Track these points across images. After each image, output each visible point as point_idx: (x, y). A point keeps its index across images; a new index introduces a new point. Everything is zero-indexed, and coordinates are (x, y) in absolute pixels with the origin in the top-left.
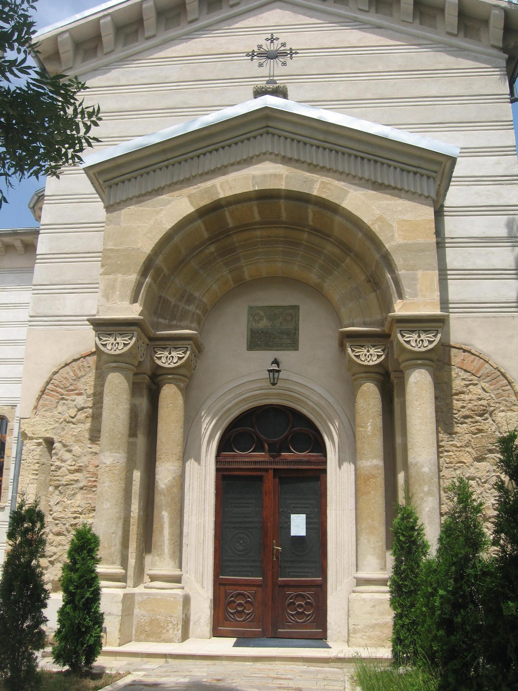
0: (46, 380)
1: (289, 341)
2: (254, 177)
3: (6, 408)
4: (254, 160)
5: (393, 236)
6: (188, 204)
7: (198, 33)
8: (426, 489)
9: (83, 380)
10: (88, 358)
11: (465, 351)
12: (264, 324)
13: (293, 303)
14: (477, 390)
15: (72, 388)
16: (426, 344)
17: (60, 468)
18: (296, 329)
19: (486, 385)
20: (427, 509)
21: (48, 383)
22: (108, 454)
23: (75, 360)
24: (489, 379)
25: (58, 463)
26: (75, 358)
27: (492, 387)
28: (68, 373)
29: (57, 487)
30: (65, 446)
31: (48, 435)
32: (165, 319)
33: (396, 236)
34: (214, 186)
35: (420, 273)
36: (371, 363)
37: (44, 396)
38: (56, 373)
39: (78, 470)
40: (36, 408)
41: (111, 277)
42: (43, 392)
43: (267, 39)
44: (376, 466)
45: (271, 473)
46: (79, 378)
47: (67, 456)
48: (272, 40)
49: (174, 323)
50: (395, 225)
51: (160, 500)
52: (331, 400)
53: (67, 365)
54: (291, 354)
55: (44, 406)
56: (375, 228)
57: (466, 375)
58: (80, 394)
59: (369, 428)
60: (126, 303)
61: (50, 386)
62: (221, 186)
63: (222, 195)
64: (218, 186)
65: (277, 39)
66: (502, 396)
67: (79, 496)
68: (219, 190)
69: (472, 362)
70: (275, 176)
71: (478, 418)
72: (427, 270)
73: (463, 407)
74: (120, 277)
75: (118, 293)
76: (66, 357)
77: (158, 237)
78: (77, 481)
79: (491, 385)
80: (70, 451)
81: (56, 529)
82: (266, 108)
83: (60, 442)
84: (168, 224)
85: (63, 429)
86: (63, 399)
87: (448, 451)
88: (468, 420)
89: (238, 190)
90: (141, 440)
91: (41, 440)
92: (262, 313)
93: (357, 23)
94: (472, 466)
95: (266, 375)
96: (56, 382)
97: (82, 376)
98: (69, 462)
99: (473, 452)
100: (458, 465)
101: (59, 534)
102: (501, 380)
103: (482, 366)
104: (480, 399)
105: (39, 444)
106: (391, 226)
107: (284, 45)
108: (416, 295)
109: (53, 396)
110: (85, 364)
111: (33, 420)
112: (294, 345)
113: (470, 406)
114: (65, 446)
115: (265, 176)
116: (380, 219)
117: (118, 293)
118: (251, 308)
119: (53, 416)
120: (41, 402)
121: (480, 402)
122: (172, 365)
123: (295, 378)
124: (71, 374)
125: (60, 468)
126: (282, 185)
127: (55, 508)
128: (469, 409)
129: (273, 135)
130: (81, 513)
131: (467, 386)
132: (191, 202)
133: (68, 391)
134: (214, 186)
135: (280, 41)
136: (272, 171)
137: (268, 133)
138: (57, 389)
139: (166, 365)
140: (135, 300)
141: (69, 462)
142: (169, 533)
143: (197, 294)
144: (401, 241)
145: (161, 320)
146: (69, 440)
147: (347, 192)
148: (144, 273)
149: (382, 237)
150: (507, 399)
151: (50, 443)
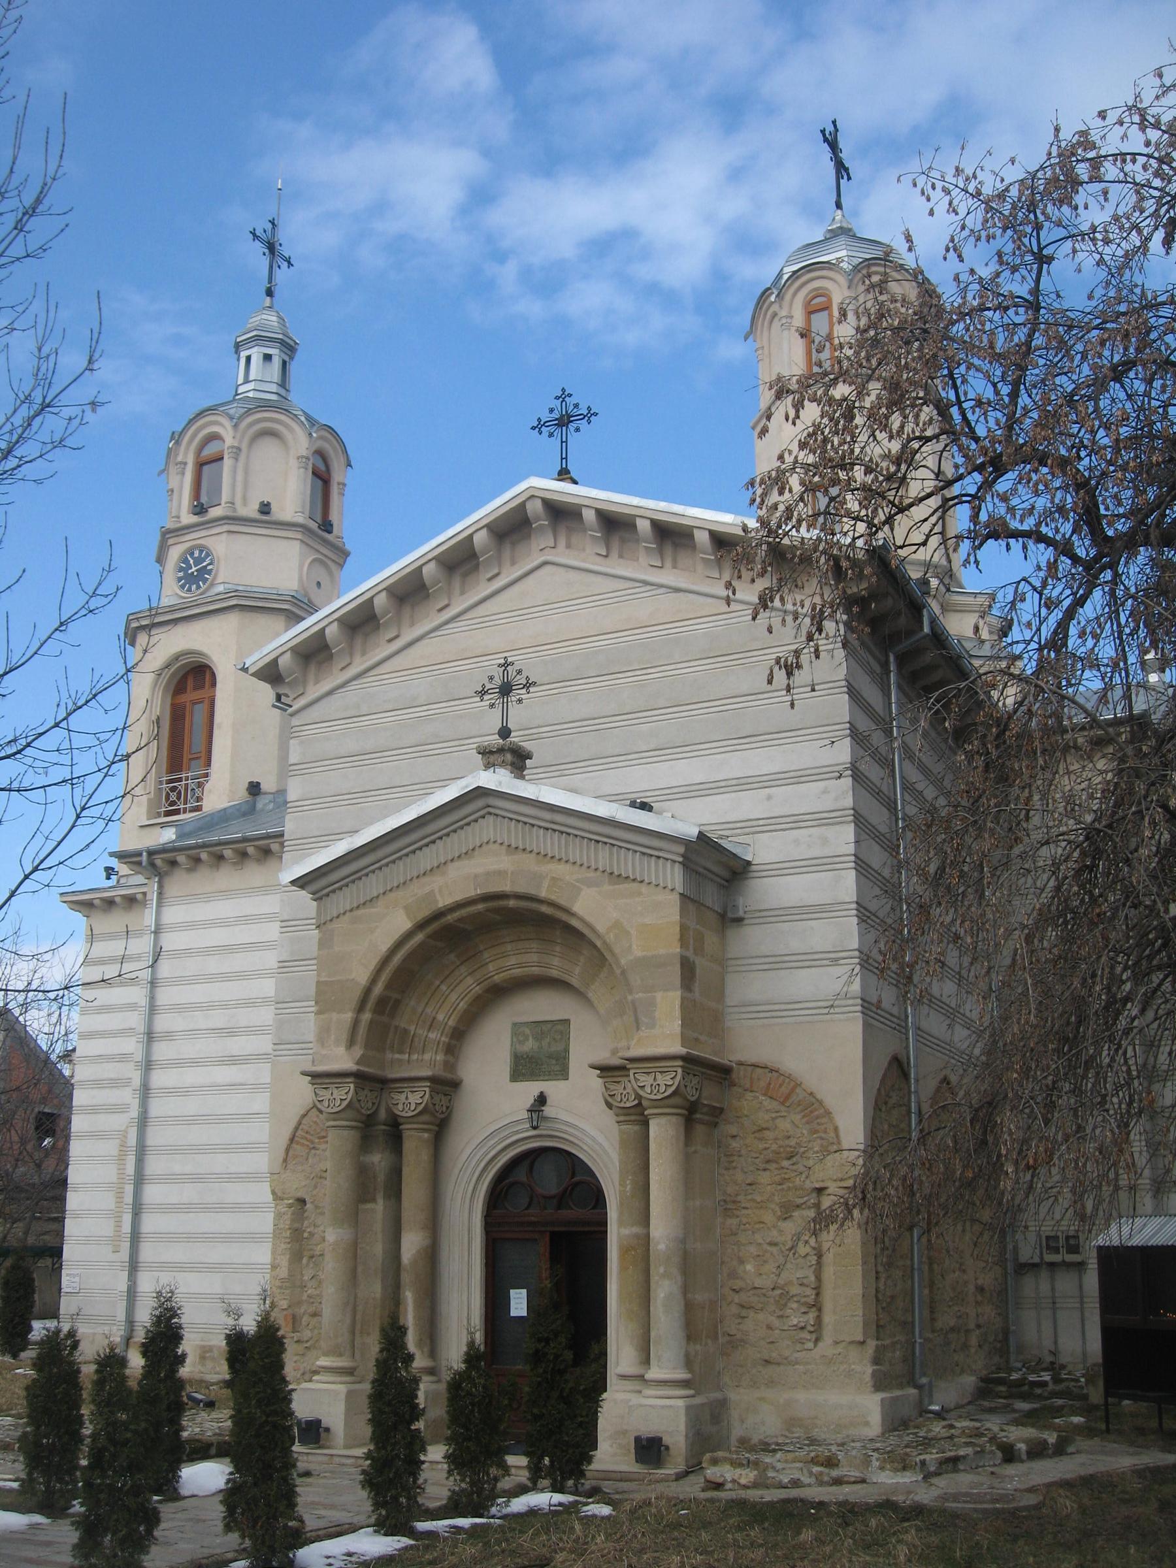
1: (557, 1068)
2: (476, 876)
4: (476, 853)
5: (630, 946)
6: (405, 917)
7: (450, 626)
8: (662, 1270)
11: (772, 1071)
12: (530, 1045)
14: (784, 1125)
16: (663, 1088)
18: (567, 1050)
19: (797, 1118)
20: (662, 1295)
21: (296, 1129)
24: (799, 1109)
27: (804, 1120)
29: (312, 1257)
30: (317, 1207)
31: (300, 1194)
32: (401, 1052)
33: (634, 947)
34: (433, 891)
35: (659, 996)
36: (628, 1105)
37: (294, 1145)
38: (304, 1116)
40: (285, 1160)
41: (326, 1016)
42: (292, 1140)
43: (500, 665)
44: (637, 1236)
48: (506, 665)
49: (415, 1057)
50: (633, 932)
51: (406, 1278)
52: (606, 1145)
54: (561, 1084)
55: (295, 1157)
56: (610, 938)
57: (775, 1105)
59: (628, 1188)
60: (341, 1050)
61: (299, 1132)
62: (440, 891)
63: (441, 905)
64: (436, 891)
65: (512, 664)
66: (816, 1132)
68: (438, 897)
69: (781, 1086)
70: (500, 873)
71: (785, 1163)
72: (667, 990)
73: (766, 1149)
74: (335, 1016)
75: (333, 1037)
77: (373, 964)
79: (804, 1117)
81: (311, 1309)
82: (479, 787)
84: (384, 946)
85: (316, 1187)
86: (314, 1148)
87: (744, 1208)
88: (773, 1166)
89: (459, 897)
90: (379, 1208)
92: (527, 1031)
93: (649, 588)
94: (774, 1227)
95: (526, 1115)
96: (305, 1128)
99: (777, 1209)
100: (757, 1226)
102: (816, 1110)
103: (793, 1090)
104: (789, 1137)
106: (628, 933)
107: (519, 672)
108: (652, 1026)
109: (303, 1145)
112: (563, 1074)
113: (774, 1147)
114: (317, 1207)
115: (488, 874)
116: (617, 925)
117: (333, 1037)
118: (515, 1024)
120: (291, 1153)
121: (787, 1142)
122: (411, 1114)
123: (563, 1116)
126: (507, 888)
128: (774, 1152)
129: (497, 815)
131: (774, 1119)
133: (319, 1138)
134: (433, 891)
135: (517, 667)
136: (495, 867)
137: (490, 813)
138: (308, 1136)
139: (404, 1114)
140: (351, 1043)
142: (414, 1317)
143: (440, 1017)
144: (639, 954)
145: (397, 1056)
147: (580, 890)
148: (361, 1008)
149: (617, 950)
150: (823, 1135)
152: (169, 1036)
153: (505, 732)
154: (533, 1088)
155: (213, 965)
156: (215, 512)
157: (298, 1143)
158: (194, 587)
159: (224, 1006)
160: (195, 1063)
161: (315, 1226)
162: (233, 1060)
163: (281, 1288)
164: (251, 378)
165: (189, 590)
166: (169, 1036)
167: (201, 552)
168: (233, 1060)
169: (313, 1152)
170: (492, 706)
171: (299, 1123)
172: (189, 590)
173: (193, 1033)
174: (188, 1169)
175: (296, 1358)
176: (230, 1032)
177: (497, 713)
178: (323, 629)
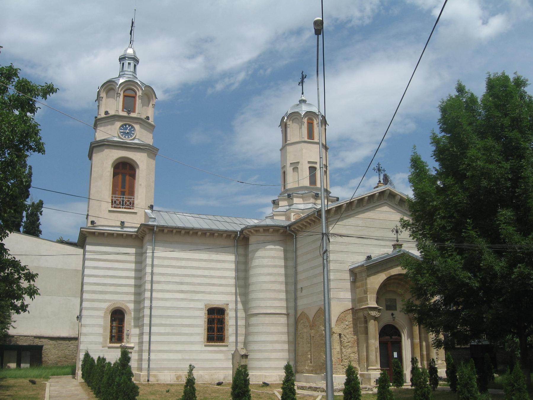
0: (338, 317)
2: (398, 269)
3: (224, 305)
9: (347, 317)
10: (348, 311)
13: (394, 298)
15: (344, 319)
17: (344, 341)
18: (396, 305)
22: (373, 340)
23: (344, 312)
25: (343, 340)
26: (345, 311)
28: (343, 315)
31: (340, 333)
38: (340, 315)
39: (348, 342)
40: (336, 325)
41: (370, 295)
42: (337, 320)
45: (390, 342)
46: (346, 316)
47: (345, 338)
53: (343, 313)
54: (396, 311)
55: (338, 324)
58: (347, 321)
63: (392, 274)
67: (349, 349)
76: (342, 311)
78: (348, 345)
80: (346, 337)
81: (345, 358)
83: (343, 334)
86: (342, 322)
91: (338, 334)
97: (347, 316)
98: (346, 340)
101: (346, 359)
105: (338, 335)
109: (339, 321)
110: (347, 312)
111: (335, 329)
112: (396, 309)
114: (344, 335)
117: (372, 300)
119: (341, 327)
124: (344, 315)
125: (344, 341)
127: (344, 352)
130: (350, 354)
132: (386, 275)
134: (390, 272)
141: (346, 340)
146: (346, 334)
151: (340, 335)
152: (159, 282)
153: (397, 241)
154: (390, 312)
155: (174, 263)
156: (133, 115)
157: (338, 321)
158: (127, 137)
159: (178, 275)
160: (168, 291)
161: (345, 340)
162: (182, 292)
163: (338, 353)
164: (124, 70)
165: (125, 137)
166: (159, 282)
167: (129, 126)
168: (182, 292)
169: (342, 323)
170: (395, 234)
171: (339, 317)
172: (125, 137)
173: (169, 282)
174: (168, 322)
175: (342, 369)
176: (182, 283)
177: (395, 236)
178: (343, 204)
